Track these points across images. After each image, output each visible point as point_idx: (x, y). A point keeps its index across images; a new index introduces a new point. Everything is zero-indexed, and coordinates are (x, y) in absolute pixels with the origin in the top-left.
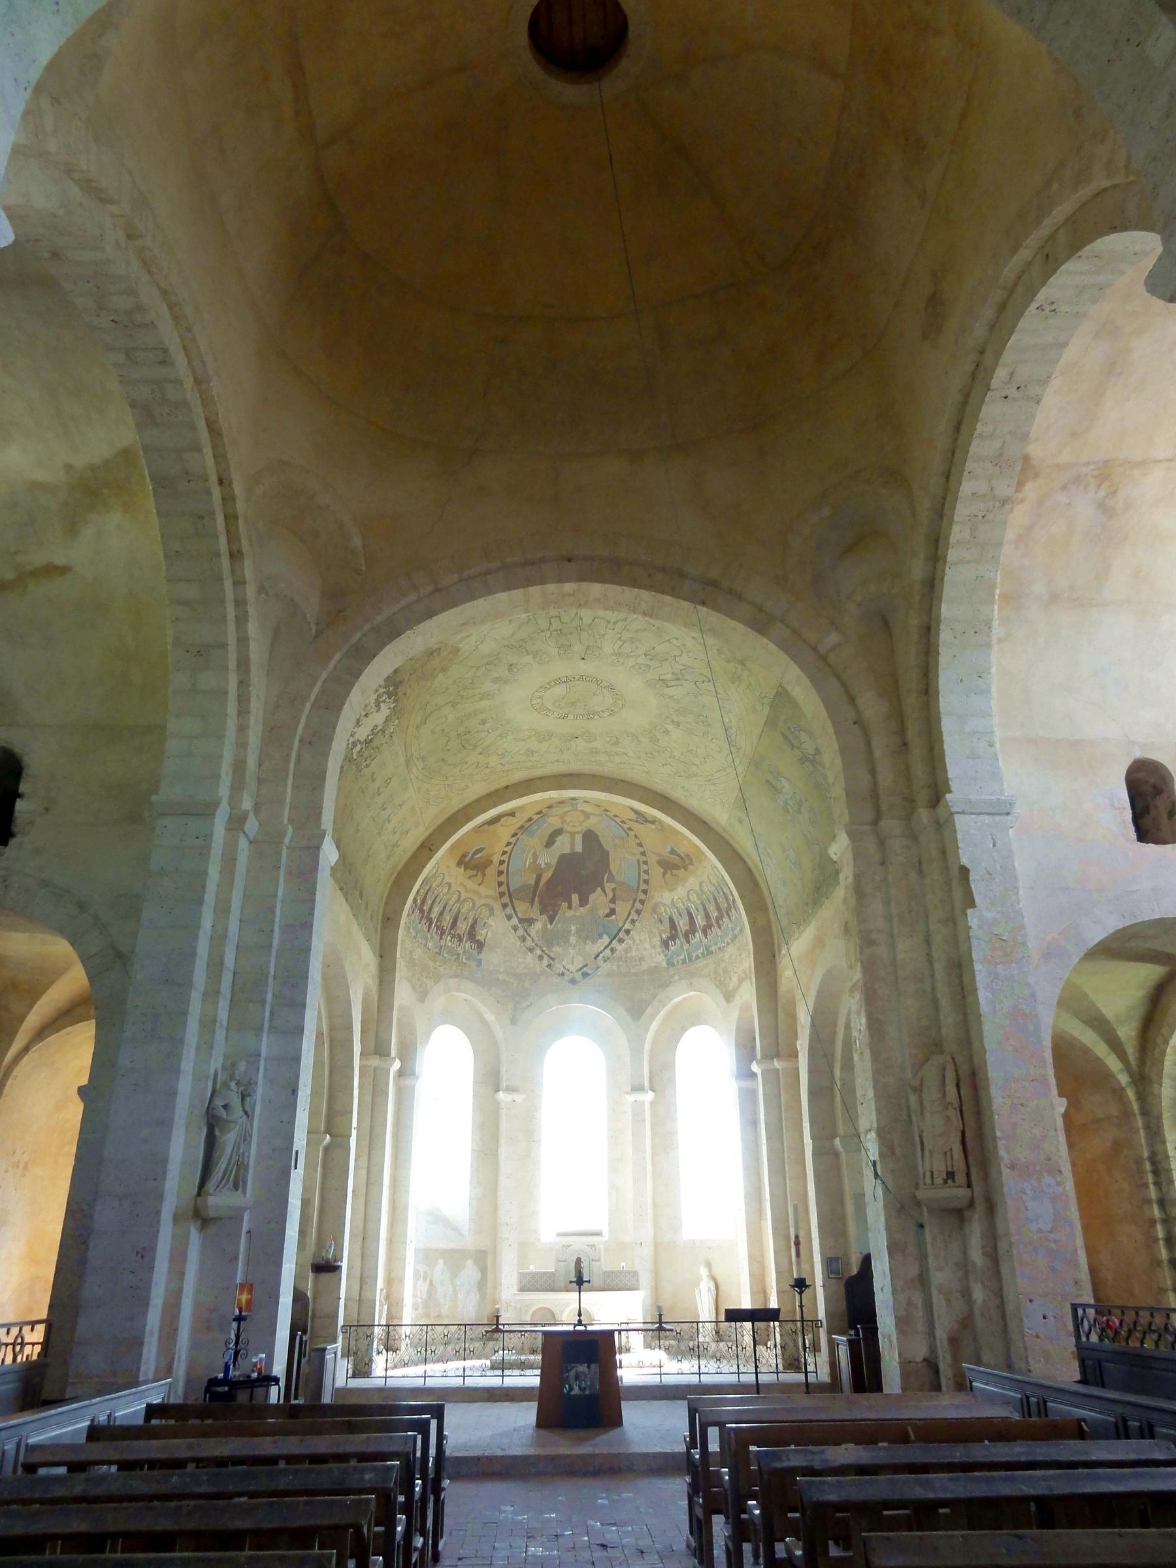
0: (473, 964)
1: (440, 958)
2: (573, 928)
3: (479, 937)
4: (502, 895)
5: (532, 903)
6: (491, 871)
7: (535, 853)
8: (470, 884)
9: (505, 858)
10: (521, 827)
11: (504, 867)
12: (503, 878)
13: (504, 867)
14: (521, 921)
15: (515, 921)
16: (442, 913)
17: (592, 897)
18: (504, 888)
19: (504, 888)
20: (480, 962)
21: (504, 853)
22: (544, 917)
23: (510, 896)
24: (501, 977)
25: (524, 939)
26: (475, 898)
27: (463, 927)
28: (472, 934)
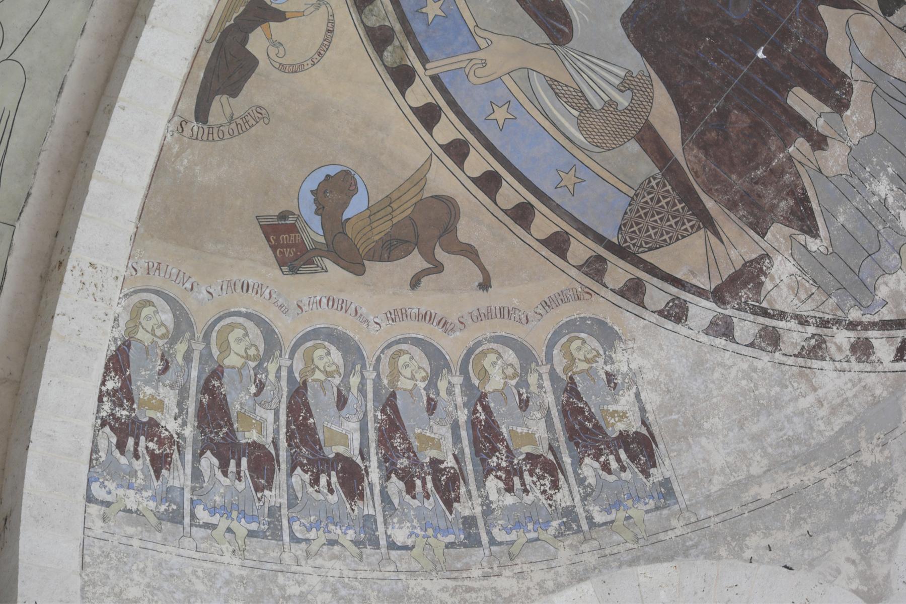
0: (637, 511)
1: (478, 554)
2: (883, 188)
3: (615, 428)
4: (595, 268)
5: (707, 222)
6: (478, 223)
7: (552, 83)
8: (428, 299)
9: (478, 162)
10: (379, 39)
11: (511, 193)
12: (545, 224)
13: (511, 193)
14: (718, 296)
15: (702, 311)
16: (392, 426)
17: (837, 52)
18: (581, 249)
19: (581, 249)
20: (666, 492)
21: (457, 151)
22: (778, 233)
23: (621, 252)
24: (766, 491)
25: (772, 339)
26: (504, 328)
27: (534, 430)
28: (582, 428)
